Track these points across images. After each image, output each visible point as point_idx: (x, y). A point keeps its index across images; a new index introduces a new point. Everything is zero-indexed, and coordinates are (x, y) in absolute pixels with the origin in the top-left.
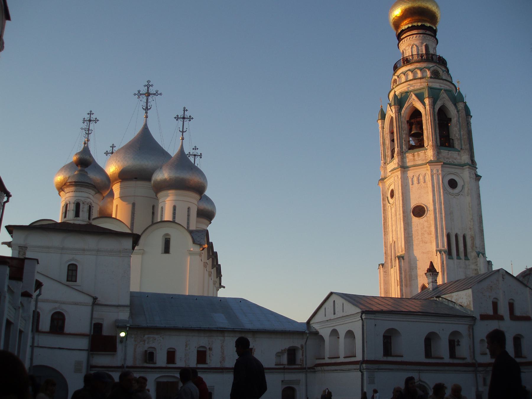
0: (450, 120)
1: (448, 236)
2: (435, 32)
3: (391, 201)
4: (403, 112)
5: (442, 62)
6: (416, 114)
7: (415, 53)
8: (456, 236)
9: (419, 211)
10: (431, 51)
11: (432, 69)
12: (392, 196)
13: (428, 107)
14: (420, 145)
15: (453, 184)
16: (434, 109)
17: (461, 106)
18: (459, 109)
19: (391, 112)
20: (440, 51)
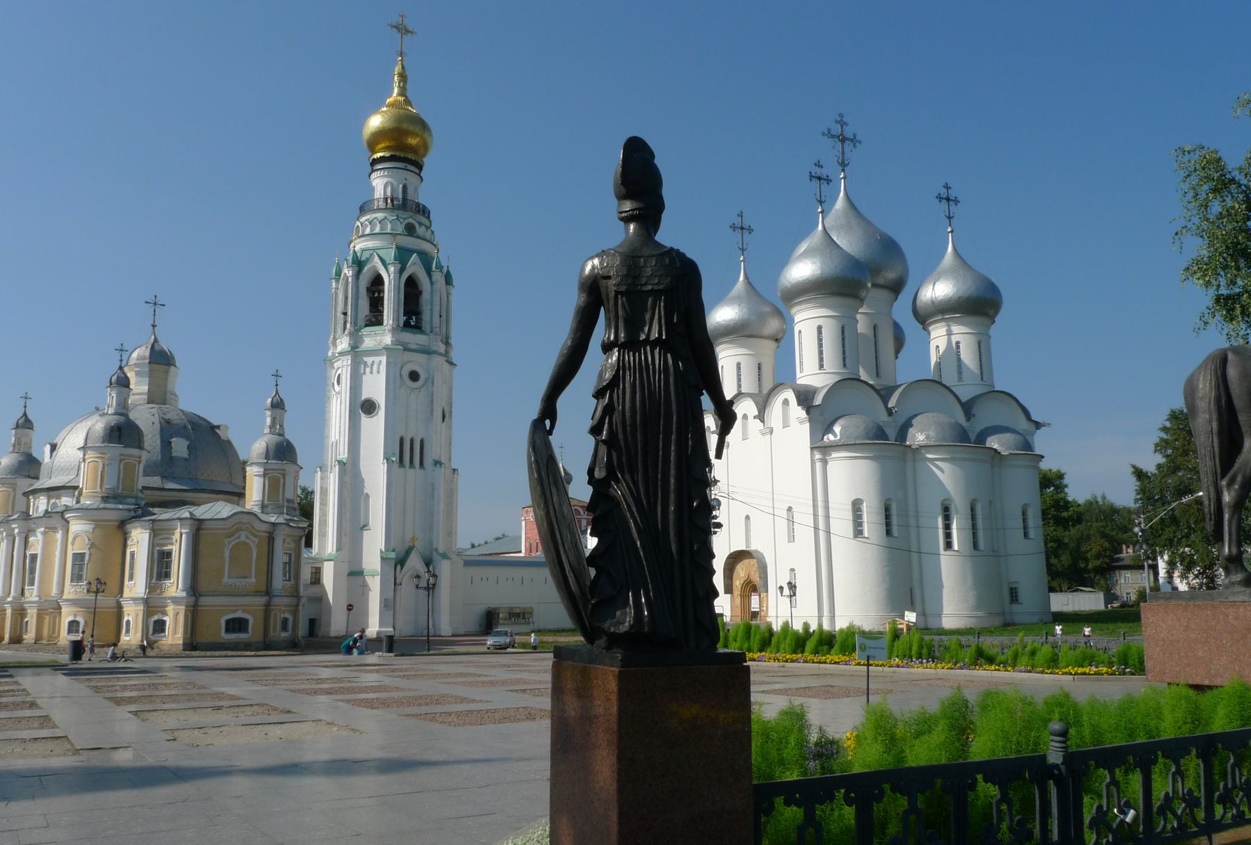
0: (421, 292)
1: (402, 440)
2: (420, 167)
3: (337, 388)
4: (361, 277)
5: (423, 211)
6: (377, 281)
7: (389, 194)
8: (412, 440)
9: (369, 407)
10: (410, 196)
11: (407, 221)
12: (338, 383)
13: (392, 276)
14: (379, 322)
15: (414, 376)
16: (400, 277)
17: (438, 277)
18: (433, 280)
19: (348, 272)
20: (424, 195)
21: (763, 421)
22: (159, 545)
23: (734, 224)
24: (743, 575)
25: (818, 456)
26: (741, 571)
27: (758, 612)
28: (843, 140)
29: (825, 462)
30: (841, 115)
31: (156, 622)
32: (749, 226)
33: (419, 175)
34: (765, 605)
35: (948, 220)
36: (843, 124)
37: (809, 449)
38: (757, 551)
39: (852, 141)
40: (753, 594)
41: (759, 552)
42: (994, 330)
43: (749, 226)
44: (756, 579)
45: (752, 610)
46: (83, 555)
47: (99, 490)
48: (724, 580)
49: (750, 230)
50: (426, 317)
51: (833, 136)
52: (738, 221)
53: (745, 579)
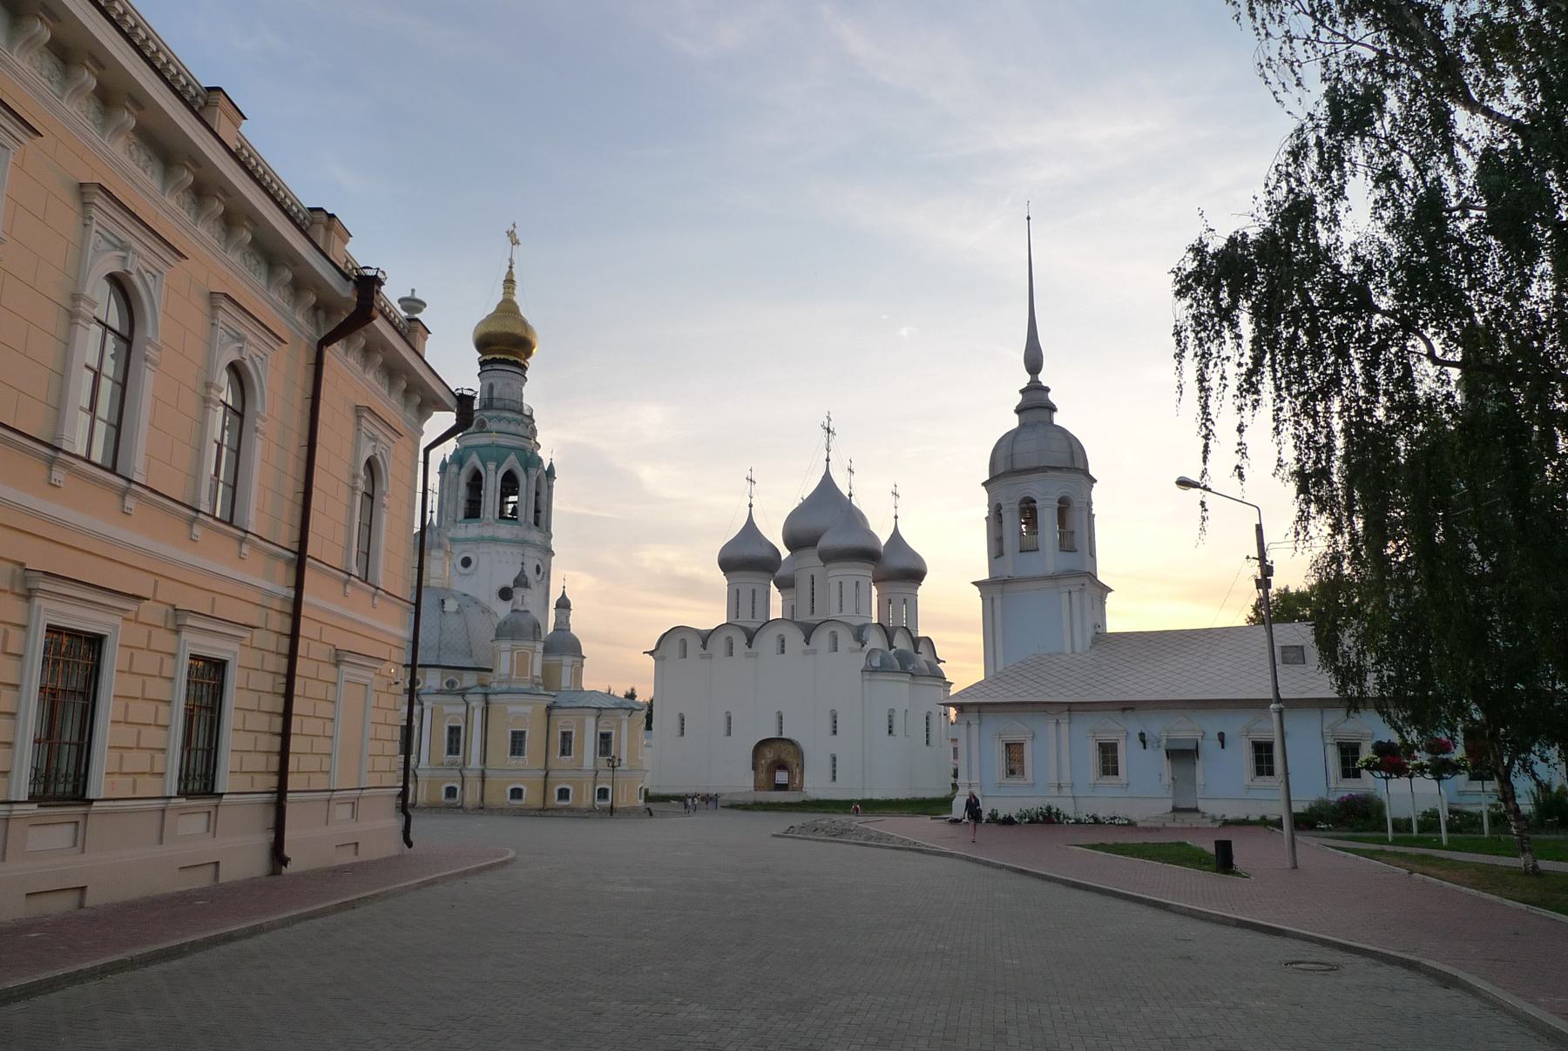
4: (499, 473)
21: (808, 644)
22: (602, 727)
25: (867, 677)
28: (829, 431)
29: (870, 680)
30: (829, 413)
31: (561, 791)
33: (524, 376)
36: (830, 420)
42: (920, 591)
44: (791, 760)
46: (523, 733)
47: (529, 677)
49: (755, 483)
50: (542, 516)
51: (824, 428)
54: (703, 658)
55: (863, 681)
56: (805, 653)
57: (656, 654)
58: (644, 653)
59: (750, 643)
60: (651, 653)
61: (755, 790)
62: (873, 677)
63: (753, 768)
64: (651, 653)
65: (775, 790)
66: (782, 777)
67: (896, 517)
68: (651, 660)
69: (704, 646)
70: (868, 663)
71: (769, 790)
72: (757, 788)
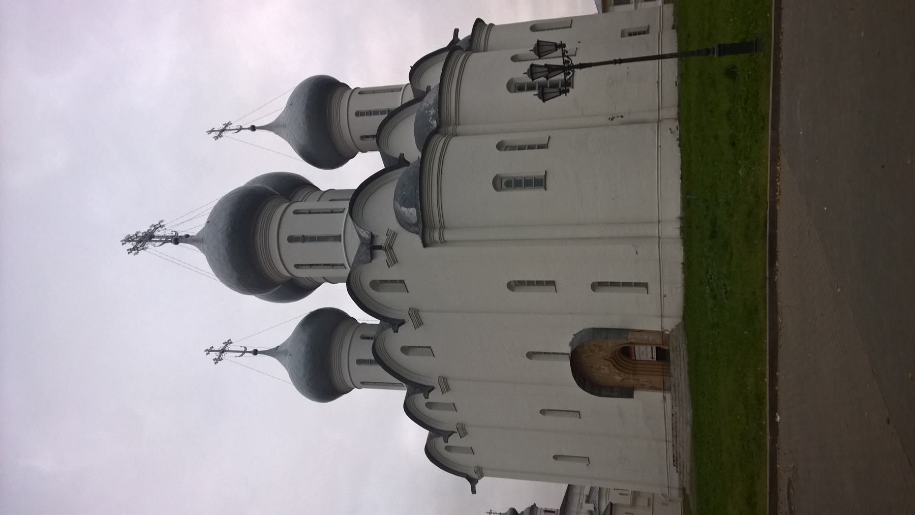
21: (403, 322)
23: (214, 360)
24: (606, 368)
26: (605, 371)
27: (656, 347)
29: (443, 227)
32: (224, 343)
34: (646, 337)
35: (242, 131)
37: (427, 249)
38: (571, 344)
39: (158, 228)
40: (633, 358)
41: (573, 339)
43: (224, 343)
45: (655, 359)
48: (613, 397)
49: (229, 342)
52: (214, 355)
53: (612, 367)
54: (466, 433)
55: (443, 242)
56: (419, 323)
57: (474, 476)
58: (474, 491)
59: (427, 390)
60: (473, 482)
61: (670, 389)
62: (437, 224)
63: (631, 396)
64: (473, 482)
65: (669, 361)
66: (645, 353)
67: (253, 128)
68: (484, 483)
69: (447, 435)
70: (417, 229)
71: (669, 366)
72: (664, 389)
